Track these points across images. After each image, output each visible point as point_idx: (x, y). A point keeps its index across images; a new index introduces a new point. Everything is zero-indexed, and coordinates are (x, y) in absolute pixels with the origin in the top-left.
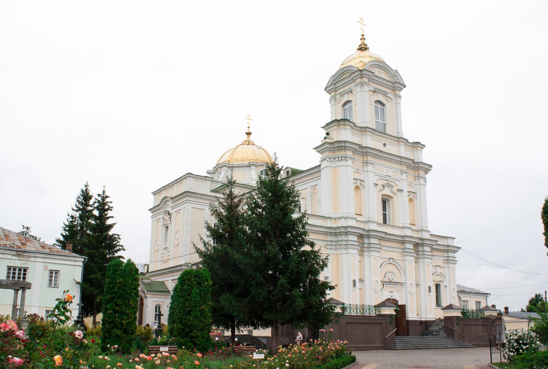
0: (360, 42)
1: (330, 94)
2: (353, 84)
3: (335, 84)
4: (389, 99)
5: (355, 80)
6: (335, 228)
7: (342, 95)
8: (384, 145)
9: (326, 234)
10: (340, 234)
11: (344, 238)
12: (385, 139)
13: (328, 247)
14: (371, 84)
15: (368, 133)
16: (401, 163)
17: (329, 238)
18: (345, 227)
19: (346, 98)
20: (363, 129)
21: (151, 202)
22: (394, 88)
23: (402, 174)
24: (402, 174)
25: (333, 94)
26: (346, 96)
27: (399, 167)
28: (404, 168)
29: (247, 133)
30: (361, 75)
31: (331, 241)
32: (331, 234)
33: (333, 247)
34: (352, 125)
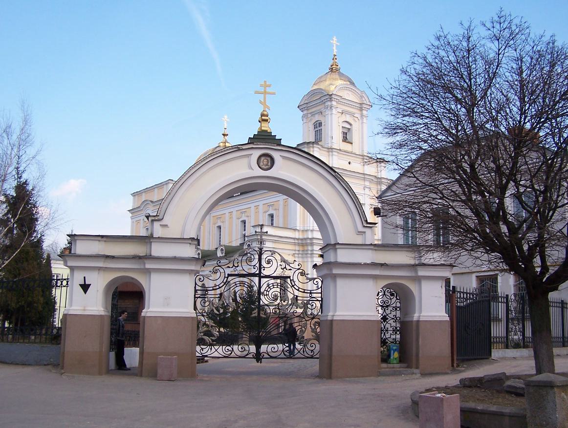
0: (331, 62)
1: (302, 111)
2: (323, 106)
3: (307, 103)
4: (355, 118)
5: (325, 103)
6: (302, 239)
7: (313, 114)
8: (349, 163)
9: (295, 244)
10: (307, 245)
11: (310, 248)
12: (349, 157)
13: (296, 255)
14: (339, 106)
15: (334, 153)
16: (364, 179)
17: (297, 248)
18: (310, 239)
19: (317, 118)
20: (331, 150)
21: (130, 203)
22: (361, 108)
23: (364, 189)
24: (364, 189)
25: (305, 112)
26: (317, 116)
27: (362, 182)
28: (367, 183)
29: (223, 135)
30: (330, 99)
31: (299, 251)
32: (299, 244)
33: (300, 255)
34: (319, 147)
